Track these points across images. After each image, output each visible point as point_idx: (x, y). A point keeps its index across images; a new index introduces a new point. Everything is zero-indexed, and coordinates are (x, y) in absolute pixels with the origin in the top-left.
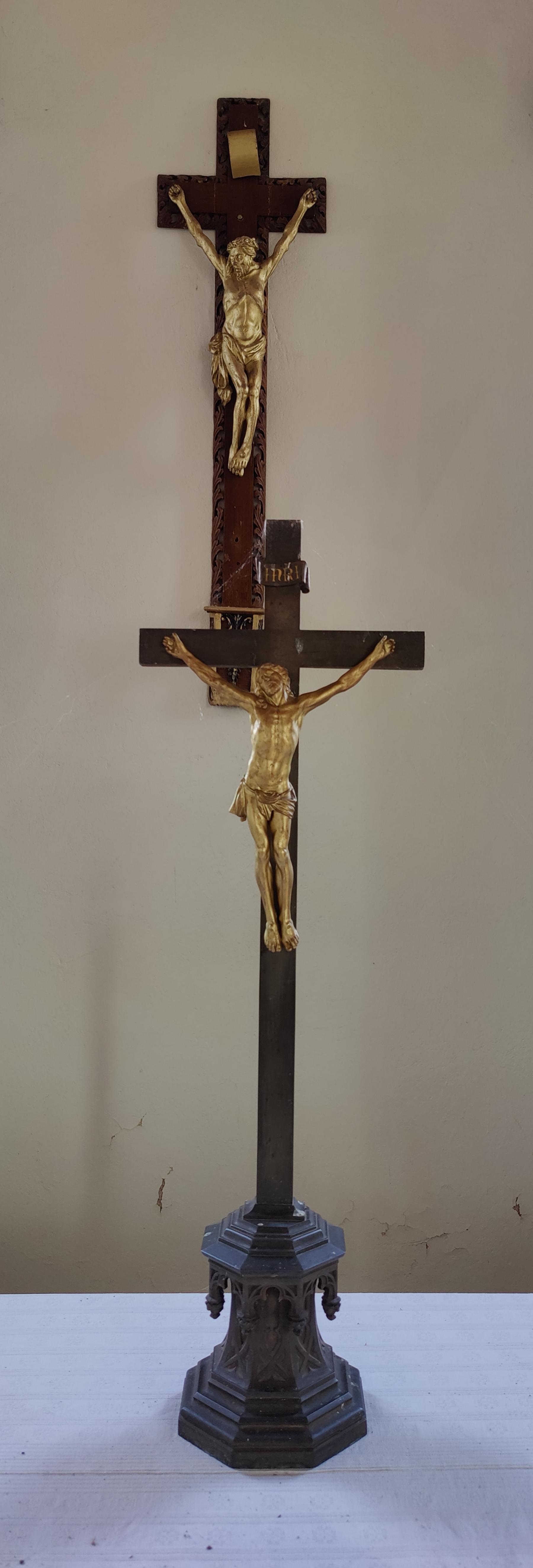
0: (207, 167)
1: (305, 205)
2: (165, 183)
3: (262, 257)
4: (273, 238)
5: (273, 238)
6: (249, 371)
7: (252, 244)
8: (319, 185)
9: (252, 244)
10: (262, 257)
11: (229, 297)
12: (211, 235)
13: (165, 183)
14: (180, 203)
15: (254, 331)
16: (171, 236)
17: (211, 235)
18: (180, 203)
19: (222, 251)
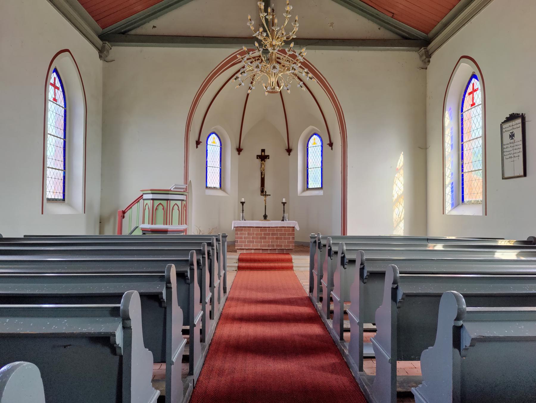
0: (260, 154)
1: (268, 157)
2: (257, 156)
3: (264, 162)
4: (265, 160)
5: (265, 160)
6: (263, 170)
7: (264, 161)
8: (268, 156)
9: (264, 161)
10: (264, 162)
11: (262, 165)
12: (260, 159)
13: (257, 156)
14: (258, 158)
15: (264, 167)
16: (258, 159)
17: (260, 159)
18: (258, 158)
19: (262, 161)
